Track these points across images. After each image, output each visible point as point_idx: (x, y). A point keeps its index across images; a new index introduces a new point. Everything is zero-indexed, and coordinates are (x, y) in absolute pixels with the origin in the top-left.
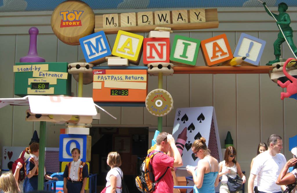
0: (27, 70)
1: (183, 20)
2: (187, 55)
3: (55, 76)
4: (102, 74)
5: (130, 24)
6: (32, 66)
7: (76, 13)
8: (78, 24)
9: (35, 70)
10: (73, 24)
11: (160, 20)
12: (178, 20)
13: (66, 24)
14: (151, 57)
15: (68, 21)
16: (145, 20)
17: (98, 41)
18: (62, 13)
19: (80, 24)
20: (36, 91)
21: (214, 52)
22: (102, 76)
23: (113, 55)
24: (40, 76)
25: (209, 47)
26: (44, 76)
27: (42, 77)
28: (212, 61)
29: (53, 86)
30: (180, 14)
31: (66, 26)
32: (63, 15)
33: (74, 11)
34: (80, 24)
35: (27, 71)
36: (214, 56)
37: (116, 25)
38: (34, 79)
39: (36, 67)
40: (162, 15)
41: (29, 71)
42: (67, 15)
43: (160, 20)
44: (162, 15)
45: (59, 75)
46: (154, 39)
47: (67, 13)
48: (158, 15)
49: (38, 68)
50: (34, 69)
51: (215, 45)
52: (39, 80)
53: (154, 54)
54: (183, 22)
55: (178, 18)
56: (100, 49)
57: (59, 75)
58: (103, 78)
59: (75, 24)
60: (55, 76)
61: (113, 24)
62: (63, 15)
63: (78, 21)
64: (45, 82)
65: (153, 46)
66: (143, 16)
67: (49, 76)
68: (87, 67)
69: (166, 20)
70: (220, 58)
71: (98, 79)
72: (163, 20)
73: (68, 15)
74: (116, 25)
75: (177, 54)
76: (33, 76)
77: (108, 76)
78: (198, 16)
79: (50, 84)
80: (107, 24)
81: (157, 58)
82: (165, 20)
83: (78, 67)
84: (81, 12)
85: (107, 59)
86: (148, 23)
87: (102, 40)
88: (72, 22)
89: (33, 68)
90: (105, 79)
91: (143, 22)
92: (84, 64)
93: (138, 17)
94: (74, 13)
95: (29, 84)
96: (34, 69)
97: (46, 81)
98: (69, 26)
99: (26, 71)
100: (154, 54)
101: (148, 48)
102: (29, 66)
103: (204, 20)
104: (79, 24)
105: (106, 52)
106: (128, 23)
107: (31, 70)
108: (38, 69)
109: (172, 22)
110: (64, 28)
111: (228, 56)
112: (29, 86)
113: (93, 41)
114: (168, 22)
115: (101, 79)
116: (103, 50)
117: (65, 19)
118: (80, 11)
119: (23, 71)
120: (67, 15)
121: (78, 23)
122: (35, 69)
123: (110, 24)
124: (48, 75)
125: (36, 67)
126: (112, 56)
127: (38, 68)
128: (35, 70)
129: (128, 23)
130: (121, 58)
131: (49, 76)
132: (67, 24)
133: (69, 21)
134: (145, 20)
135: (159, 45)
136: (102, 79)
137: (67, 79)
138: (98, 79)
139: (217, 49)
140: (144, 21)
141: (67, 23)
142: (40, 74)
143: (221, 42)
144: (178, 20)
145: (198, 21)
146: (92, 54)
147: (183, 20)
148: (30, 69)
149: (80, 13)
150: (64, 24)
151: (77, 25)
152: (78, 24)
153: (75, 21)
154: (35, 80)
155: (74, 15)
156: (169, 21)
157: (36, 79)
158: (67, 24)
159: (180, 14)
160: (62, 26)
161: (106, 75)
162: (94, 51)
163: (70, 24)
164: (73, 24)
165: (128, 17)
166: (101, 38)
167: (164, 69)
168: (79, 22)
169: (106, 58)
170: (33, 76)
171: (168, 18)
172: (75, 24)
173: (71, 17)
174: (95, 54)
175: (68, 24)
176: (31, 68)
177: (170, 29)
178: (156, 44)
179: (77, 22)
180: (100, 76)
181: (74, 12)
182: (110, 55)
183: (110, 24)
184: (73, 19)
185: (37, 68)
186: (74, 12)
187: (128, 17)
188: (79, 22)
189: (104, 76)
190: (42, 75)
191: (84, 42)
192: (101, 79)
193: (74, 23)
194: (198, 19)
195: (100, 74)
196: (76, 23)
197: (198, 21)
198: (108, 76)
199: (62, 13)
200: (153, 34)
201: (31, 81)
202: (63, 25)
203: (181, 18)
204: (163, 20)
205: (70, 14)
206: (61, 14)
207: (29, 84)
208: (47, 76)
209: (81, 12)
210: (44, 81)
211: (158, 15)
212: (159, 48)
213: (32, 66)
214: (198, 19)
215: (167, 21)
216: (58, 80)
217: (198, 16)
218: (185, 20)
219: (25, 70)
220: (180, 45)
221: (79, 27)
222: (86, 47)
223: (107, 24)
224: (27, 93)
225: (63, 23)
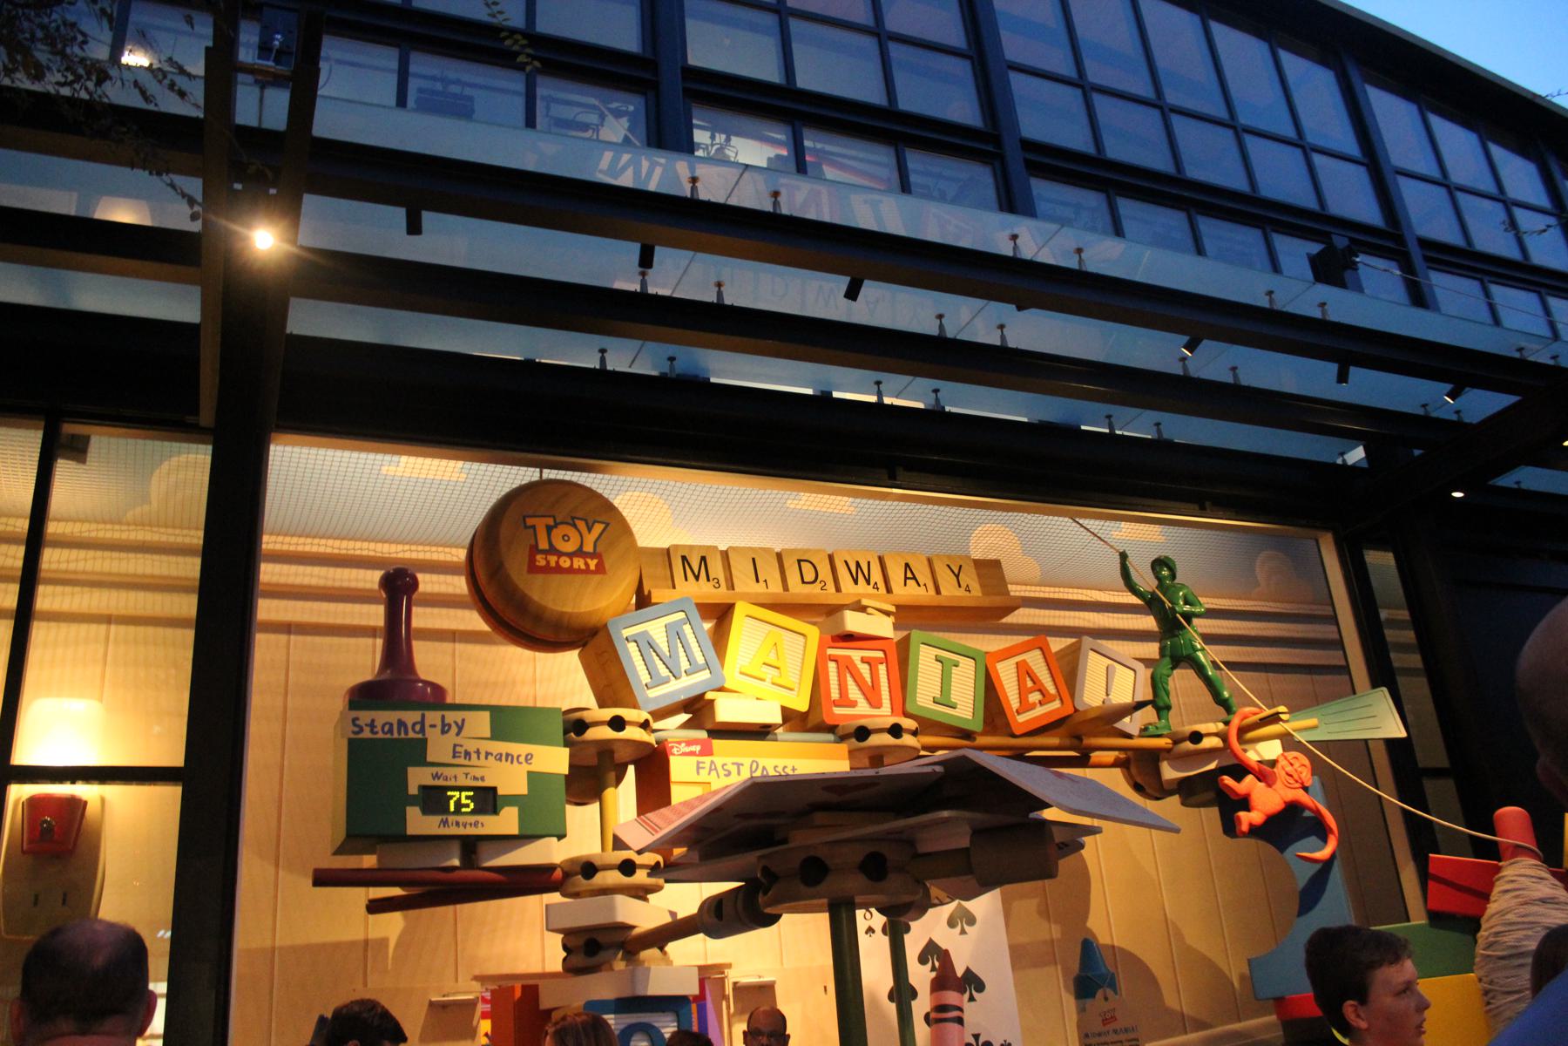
0: (399, 733)
1: (919, 585)
2: (954, 698)
3: (507, 760)
4: (702, 753)
5: (762, 583)
6: (423, 716)
7: (581, 525)
8: (592, 567)
9: (443, 732)
10: (576, 566)
11: (856, 582)
12: (905, 585)
13: (548, 562)
14: (845, 701)
15: (553, 550)
16: (809, 576)
17: (674, 633)
18: (530, 521)
19: (600, 569)
20: (445, 823)
21: (1023, 693)
22: (712, 762)
23: (726, 686)
24: (454, 757)
25: (1007, 674)
26: (470, 759)
27: (461, 761)
28: (1021, 718)
29: (512, 800)
30: (907, 565)
31: (547, 570)
32: (533, 527)
33: (573, 518)
34: (600, 569)
35: (403, 736)
36: (1025, 706)
37: (718, 583)
38: (434, 770)
39: (446, 722)
40: (858, 565)
41: (411, 735)
42: (549, 529)
43: (856, 582)
44: (858, 565)
45: (519, 756)
46: (849, 638)
47: (551, 522)
48: (846, 562)
49: (456, 723)
50: (433, 726)
51: (1024, 671)
52: (455, 777)
53: (854, 692)
54: (922, 591)
55: (906, 578)
56: (685, 665)
57: (519, 756)
58: (716, 769)
59: (583, 567)
60: (507, 760)
61: (708, 580)
62: (533, 527)
63: (593, 555)
64: (479, 784)
65: (846, 667)
66: (799, 561)
67: (486, 758)
68: (645, 725)
69: (872, 583)
70: (1039, 711)
71: (698, 773)
72: (861, 578)
73: (555, 530)
74: (717, 585)
75: (925, 693)
76: (429, 759)
77: (733, 764)
78: (957, 576)
79: (500, 792)
80: (686, 580)
81: (863, 708)
82: (868, 583)
83: (618, 723)
84: (603, 526)
85: (712, 702)
86: (818, 586)
87: (687, 629)
88: (571, 555)
89: (427, 724)
90: (726, 775)
91: (803, 582)
92: (639, 715)
93: (786, 565)
94: (575, 526)
95: (413, 790)
96: (433, 726)
97: (483, 779)
98: (558, 569)
99: (396, 735)
100: (854, 692)
101: (832, 666)
102: (411, 717)
103: (976, 591)
104: (597, 565)
105: (705, 675)
106: (757, 581)
107: (422, 730)
108: (454, 729)
109: (889, 590)
110: (540, 578)
111: (1056, 704)
112: (412, 801)
113: (656, 629)
114: (878, 589)
115: (709, 774)
116: (694, 669)
117: (544, 545)
118: (595, 522)
119: (381, 735)
120: (549, 529)
121: (593, 564)
122: (439, 727)
123: (697, 578)
124: (482, 756)
125: (446, 722)
126: (721, 689)
127: (456, 723)
128: (443, 732)
129: (757, 581)
130: (757, 699)
131: (486, 758)
132: (553, 564)
133: (560, 554)
134: (809, 576)
135: (863, 660)
136: (714, 773)
137: (567, 772)
138: (698, 773)
139: (1030, 684)
140: (805, 580)
141: (553, 559)
142: (454, 752)
143: (1035, 659)
144: (905, 585)
145: (961, 592)
146: (658, 681)
147: (919, 585)
148: (418, 728)
149: (598, 528)
150: (541, 561)
151: (587, 571)
152: (592, 567)
153: (580, 553)
154: (436, 776)
155: (577, 533)
156: (881, 585)
157: (440, 770)
158: (553, 564)
159: (907, 565)
160: (533, 569)
161: (719, 761)
162: (664, 672)
163: (565, 563)
164: (576, 566)
165: (754, 559)
166: (682, 622)
167: (907, 740)
168: (595, 561)
169: (709, 696)
170: (429, 759)
171: (876, 576)
172: (583, 567)
173: (566, 538)
174: (666, 681)
175: (557, 563)
176: (422, 722)
177: (893, 609)
178: (856, 655)
179: (589, 561)
180: (704, 763)
181: (577, 522)
182: (717, 686)
183: (697, 578)
184: (570, 547)
185: (450, 726)
186: (577, 522)
187: (754, 559)
188: (595, 561)
189: (707, 759)
190: (463, 755)
191: (626, 633)
192: (709, 774)
193: (579, 563)
194: (960, 586)
195: (692, 754)
196: (587, 564)
197: (961, 592)
198: (733, 764)
199: (530, 521)
200: (854, 622)
201: (418, 778)
202: (537, 563)
203: (914, 578)
204: (861, 578)
205: (561, 527)
206: (528, 524)
207: (413, 790)
208: (479, 758)
209: (603, 526)
210: (475, 778)
211: (846, 562)
212: (864, 670)
213: (423, 716)
214: (960, 586)
215: (876, 583)
216: (533, 777)
217: (957, 576)
218: (925, 585)
219: (391, 731)
220: (926, 661)
221: (597, 578)
222: (632, 647)
223: (686, 580)
224: (405, 831)
225: (539, 557)
